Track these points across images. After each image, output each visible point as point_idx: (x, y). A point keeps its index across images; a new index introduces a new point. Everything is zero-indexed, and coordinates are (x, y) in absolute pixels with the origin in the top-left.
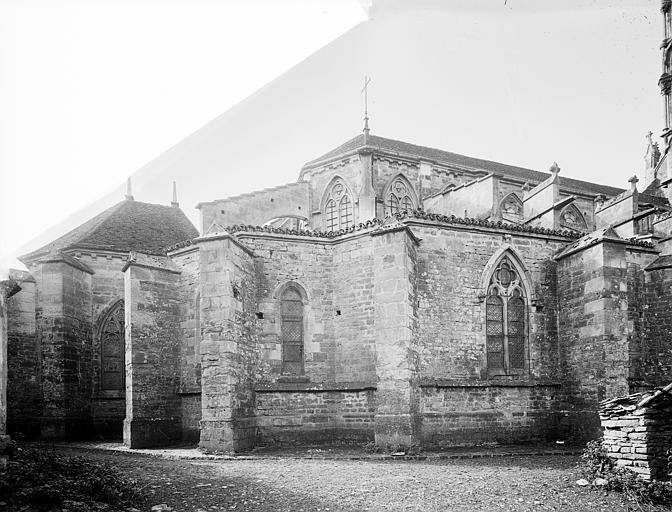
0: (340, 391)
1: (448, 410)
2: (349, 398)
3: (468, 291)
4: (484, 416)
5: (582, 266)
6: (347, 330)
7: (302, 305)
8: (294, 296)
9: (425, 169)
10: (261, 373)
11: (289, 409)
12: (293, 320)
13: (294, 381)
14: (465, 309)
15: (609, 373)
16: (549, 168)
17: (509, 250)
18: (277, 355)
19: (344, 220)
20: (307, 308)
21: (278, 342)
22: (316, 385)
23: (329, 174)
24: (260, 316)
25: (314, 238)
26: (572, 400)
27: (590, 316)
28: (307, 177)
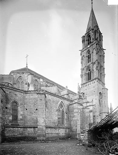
0: (27, 128)
1: (51, 132)
2: (29, 129)
3: (55, 108)
4: (57, 133)
5: (73, 107)
6: (29, 114)
7: (17, 107)
8: (15, 104)
9: (41, 80)
10: (6, 122)
11: (14, 132)
12: (15, 110)
13: (15, 125)
14: (54, 112)
15: (78, 126)
16: (66, 86)
17: (62, 101)
18: (11, 118)
19: (22, 87)
20: (19, 107)
21: (11, 115)
22: (20, 126)
23: (18, 75)
24: (6, 108)
25: (21, 91)
26: (71, 131)
27: (75, 116)
28: (12, 74)
